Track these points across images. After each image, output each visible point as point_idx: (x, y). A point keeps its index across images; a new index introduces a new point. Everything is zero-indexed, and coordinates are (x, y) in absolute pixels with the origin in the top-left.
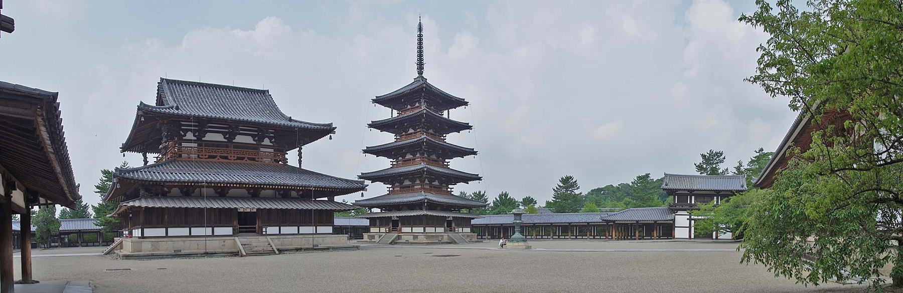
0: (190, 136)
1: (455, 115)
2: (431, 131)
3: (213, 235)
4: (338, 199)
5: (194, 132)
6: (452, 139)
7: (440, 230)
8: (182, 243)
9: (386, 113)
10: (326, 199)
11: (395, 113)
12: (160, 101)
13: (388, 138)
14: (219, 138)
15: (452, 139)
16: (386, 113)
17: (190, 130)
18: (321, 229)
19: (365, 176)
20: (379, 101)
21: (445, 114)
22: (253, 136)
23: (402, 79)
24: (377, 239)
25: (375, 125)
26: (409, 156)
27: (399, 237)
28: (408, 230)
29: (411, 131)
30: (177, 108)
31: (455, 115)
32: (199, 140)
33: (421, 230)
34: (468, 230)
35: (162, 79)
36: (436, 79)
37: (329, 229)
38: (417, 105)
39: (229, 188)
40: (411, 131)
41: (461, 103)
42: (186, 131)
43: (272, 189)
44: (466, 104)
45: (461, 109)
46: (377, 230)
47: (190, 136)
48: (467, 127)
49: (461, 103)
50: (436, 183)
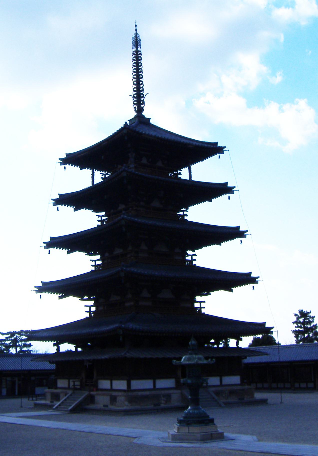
1: (202, 172)
2: (156, 204)
7: (168, 383)
23: (109, 118)
26: (118, 251)
27: (91, 399)
29: (122, 207)
31: (202, 172)
41: (210, 150)
45: (212, 160)
49: (210, 150)
50: (166, 294)
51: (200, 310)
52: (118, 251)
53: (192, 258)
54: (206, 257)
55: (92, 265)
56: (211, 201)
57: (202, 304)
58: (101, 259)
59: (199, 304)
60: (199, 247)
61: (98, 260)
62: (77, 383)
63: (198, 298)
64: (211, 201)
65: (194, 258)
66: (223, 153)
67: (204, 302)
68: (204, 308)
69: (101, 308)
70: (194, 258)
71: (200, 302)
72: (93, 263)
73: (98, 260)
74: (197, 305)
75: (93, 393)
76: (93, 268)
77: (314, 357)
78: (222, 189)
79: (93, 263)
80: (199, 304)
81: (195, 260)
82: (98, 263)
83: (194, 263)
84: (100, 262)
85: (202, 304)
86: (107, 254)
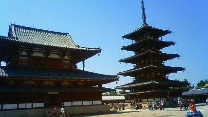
0: (24, 53)
1: (165, 39)
4: (104, 86)
5: (26, 52)
6: (164, 51)
9: (129, 42)
11: (134, 42)
12: (10, 34)
13: (132, 54)
14: (41, 55)
15: (164, 51)
17: (25, 51)
18: (95, 102)
19: (120, 74)
20: (125, 37)
21: (160, 39)
22: (59, 55)
23: (136, 25)
25: (124, 48)
26: (143, 62)
29: (142, 49)
30: (17, 38)
31: (165, 39)
32: (29, 56)
35: (12, 25)
37: (99, 102)
39: (45, 81)
42: (22, 51)
43: (67, 81)
44: (170, 32)
47: (24, 53)
48: (172, 43)
50: (159, 74)
52: (143, 62)
54: (168, 63)
69: (138, 79)
77: (206, 92)
78: (172, 43)
86: (138, 63)
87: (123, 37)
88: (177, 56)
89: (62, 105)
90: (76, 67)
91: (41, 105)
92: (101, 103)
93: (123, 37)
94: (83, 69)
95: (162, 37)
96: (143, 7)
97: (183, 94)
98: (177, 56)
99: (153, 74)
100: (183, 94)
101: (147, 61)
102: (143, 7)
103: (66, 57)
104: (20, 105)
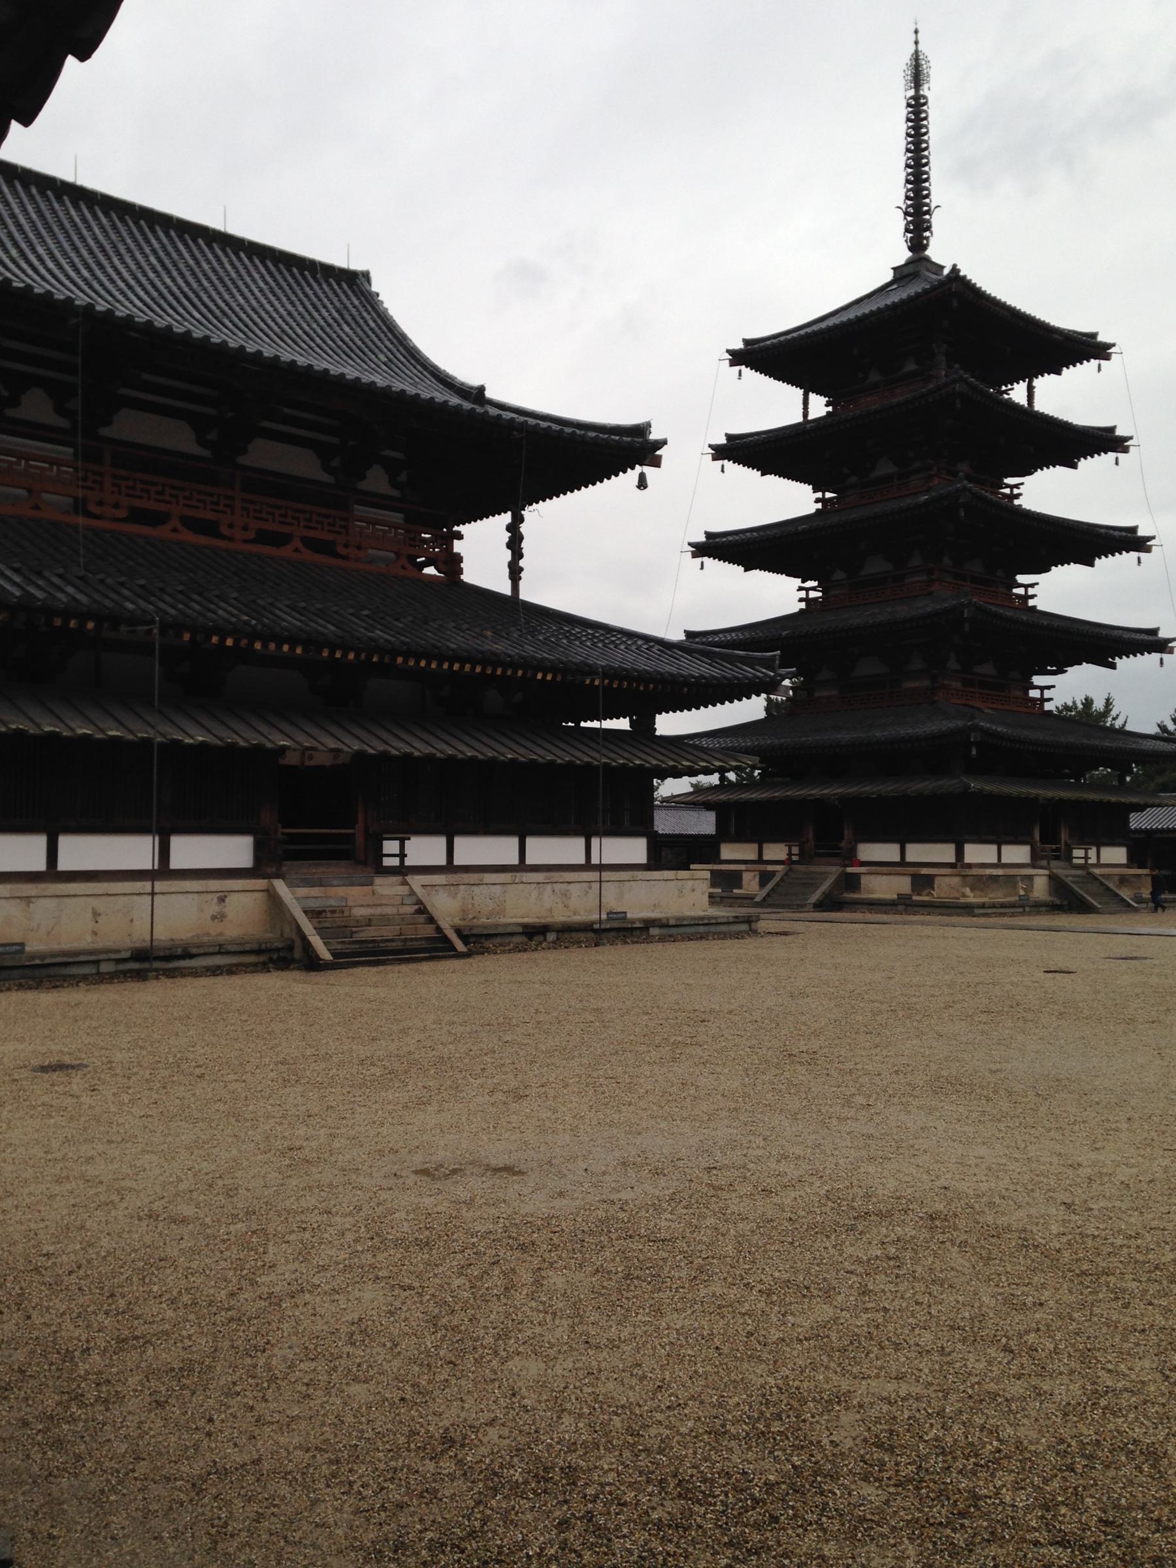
3: (163, 871)
4: (669, 724)
7: (1017, 854)
8: (14, 910)
9: (779, 405)
10: (622, 724)
13: (790, 500)
16: (779, 405)
23: (843, 265)
24: (750, 884)
26: (876, 566)
27: (852, 882)
28: (888, 852)
29: (884, 468)
33: (943, 853)
34: (1116, 855)
36: (997, 252)
37: (634, 850)
38: (911, 366)
40: (884, 468)
46: (747, 851)
51: (1042, 706)
52: (876, 566)
53: (1026, 591)
54: (1059, 591)
55: (801, 600)
56: (1074, 466)
57: (1046, 691)
58: (824, 586)
59: (1038, 691)
60: (1044, 569)
61: (814, 589)
62: (795, 850)
63: (1038, 680)
64: (1074, 466)
65: (1031, 591)
66: (1107, 357)
67: (1049, 687)
68: (1049, 700)
70: (1031, 591)
71: (1042, 689)
72: (803, 594)
73: (814, 589)
74: (1034, 694)
75: (850, 870)
76: (803, 605)
79: (803, 594)
80: (1038, 691)
81: (1033, 597)
82: (813, 594)
83: (1031, 603)
84: (820, 594)
85: (1046, 691)
86: (839, 575)
87: (738, 358)
88: (1128, 541)
89: (381, 855)
90: (453, 563)
91: (234, 850)
92: (643, 859)
93: (738, 358)
94: (505, 589)
95: (1038, 382)
96: (917, 109)
97: (1137, 821)
98: (1128, 541)
99: (953, 664)
100: (1137, 821)
101: (916, 561)
102: (917, 109)
103: (376, 481)
104: (66, 843)
